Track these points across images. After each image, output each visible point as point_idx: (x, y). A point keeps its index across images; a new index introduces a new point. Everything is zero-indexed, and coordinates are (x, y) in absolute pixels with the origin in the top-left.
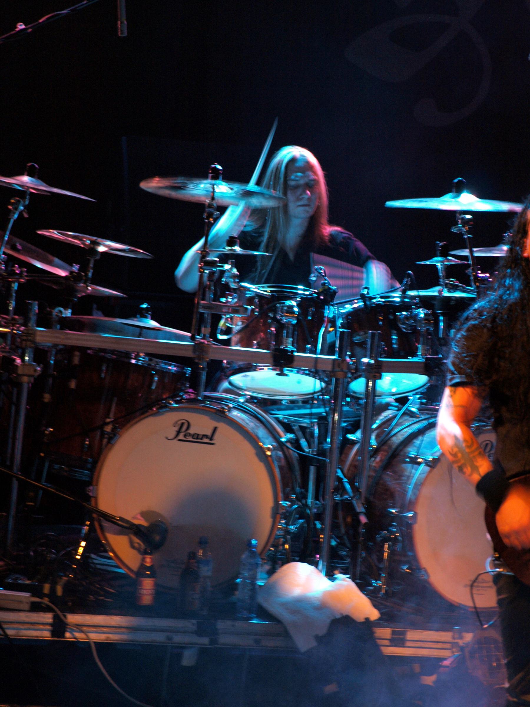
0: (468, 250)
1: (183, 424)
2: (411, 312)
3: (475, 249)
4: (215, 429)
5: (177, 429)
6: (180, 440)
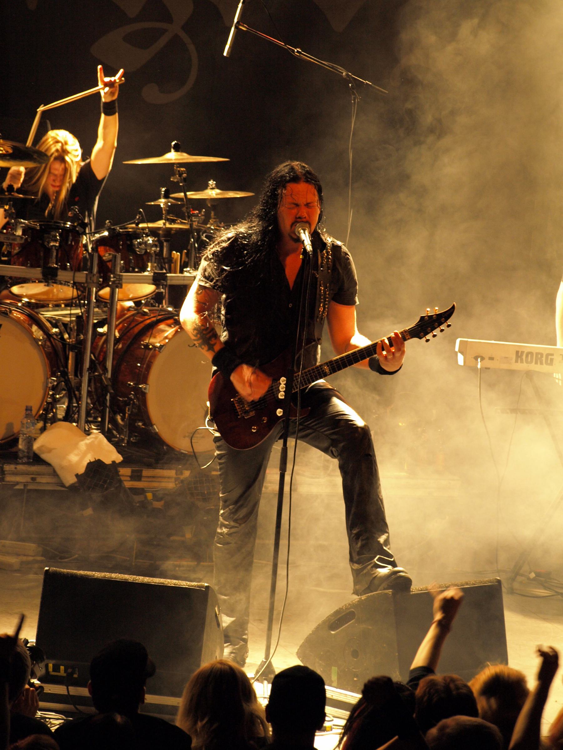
2: (143, 240)
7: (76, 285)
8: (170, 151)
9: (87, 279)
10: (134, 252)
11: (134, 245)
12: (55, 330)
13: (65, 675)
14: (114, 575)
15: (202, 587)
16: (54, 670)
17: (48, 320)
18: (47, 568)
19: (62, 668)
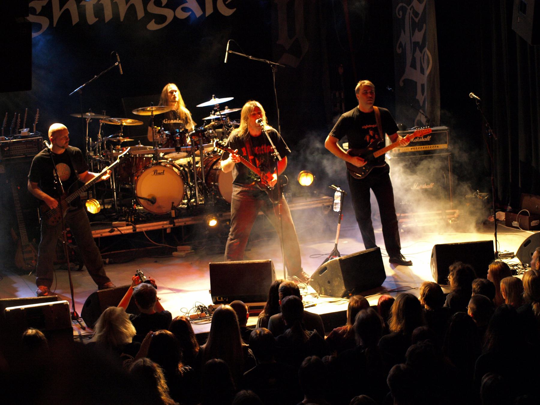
0: (219, 112)
1: (155, 171)
3: (220, 112)
4: (164, 171)
5: (154, 172)
6: (155, 175)
7: (187, 152)
8: (212, 98)
9: (191, 149)
10: (205, 137)
12: (182, 168)
13: (223, 300)
14: (235, 262)
15: (268, 261)
17: (178, 165)
18: (210, 263)
19: (222, 298)
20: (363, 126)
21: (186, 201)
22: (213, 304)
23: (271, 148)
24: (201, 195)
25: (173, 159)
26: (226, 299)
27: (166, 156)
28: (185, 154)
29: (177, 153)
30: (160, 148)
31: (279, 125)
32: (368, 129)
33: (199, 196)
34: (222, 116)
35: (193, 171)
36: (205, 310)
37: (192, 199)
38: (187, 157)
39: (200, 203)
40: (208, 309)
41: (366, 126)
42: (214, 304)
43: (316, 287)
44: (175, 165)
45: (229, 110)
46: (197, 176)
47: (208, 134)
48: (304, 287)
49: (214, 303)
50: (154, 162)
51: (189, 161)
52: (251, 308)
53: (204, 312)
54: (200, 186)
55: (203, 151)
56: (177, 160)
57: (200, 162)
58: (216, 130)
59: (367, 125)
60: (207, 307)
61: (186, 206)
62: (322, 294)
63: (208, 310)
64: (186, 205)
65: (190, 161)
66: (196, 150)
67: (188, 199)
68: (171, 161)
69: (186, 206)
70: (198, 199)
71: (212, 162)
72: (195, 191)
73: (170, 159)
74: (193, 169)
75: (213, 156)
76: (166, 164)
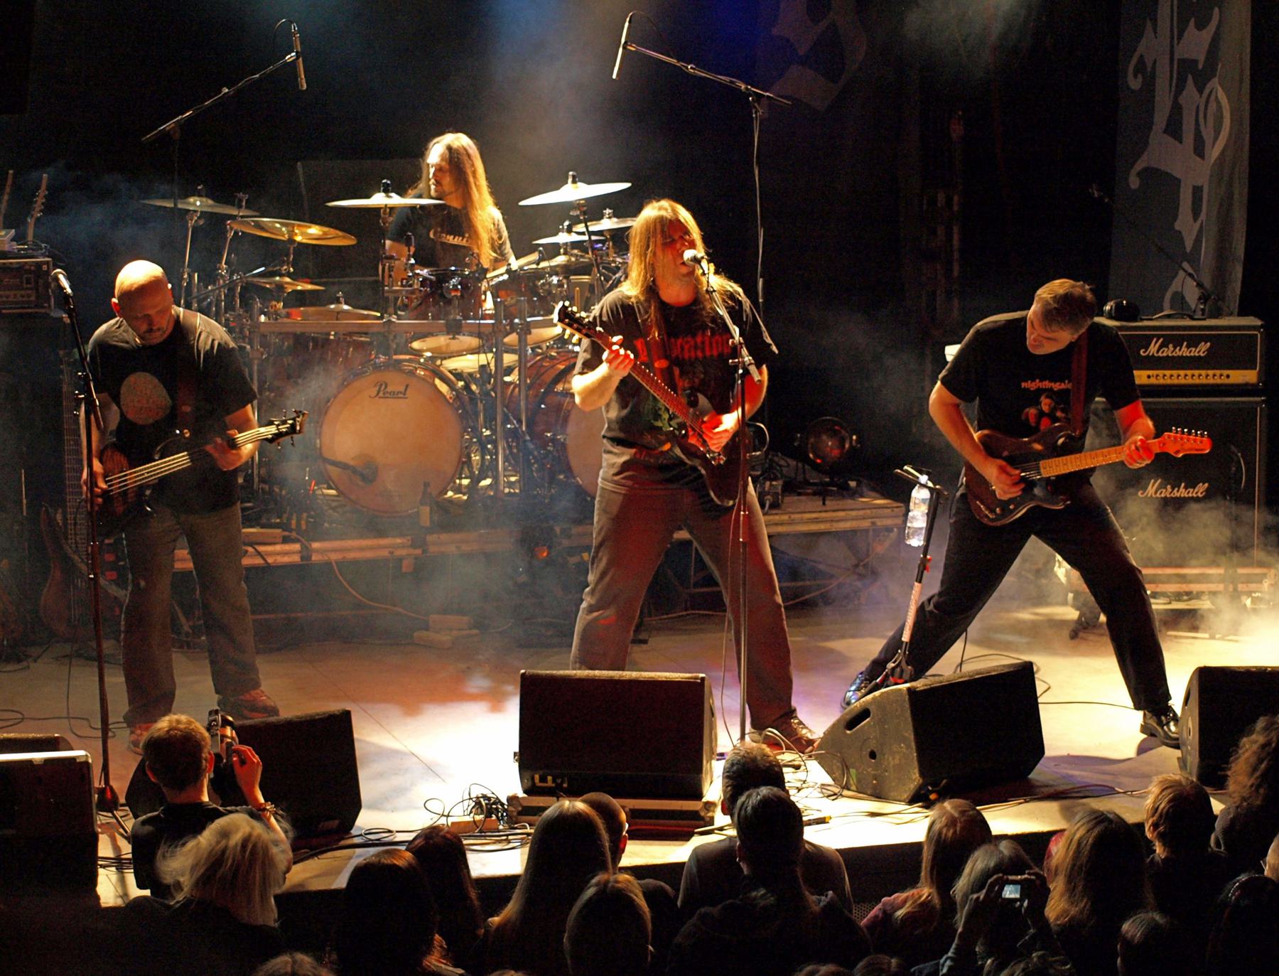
0: (583, 225)
1: (381, 385)
3: (588, 224)
4: (407, 386)
5: (377, 388)
7: (479, 336)
10: (537, 294)
11: (537, 287)
12: (461, 384)
13: (554, 785)
14: (597, 673)
15: (696, 678)
16: (540, 781)
17: (450, 372)
18: (523, 671)
19: (550, 778)
20: (1026, 381)
21: (465, 482)
22: (521, 794)
23: (731, 341)
24: (513, 467)
25: (435, 355)
26: (562, 782)
27: (416, 345)
28: (474, 342)
29: (451, 336)
30: (399, 318)
31: (761, 277)
32: (1039, 392)
33: (505, 469)
34: (594, 238)
35: (493, 394)
36: (497, 809)
37: (485, 479)
38: (478, 353)
39: (507, 490)
40: (506, 807)
41: (1034, 383)
42: (525, 795)
43: (834, 767)
44: (442, 372)
45: (615, 220)
46: (505, 409)
47: (547, 287)
48: (796, 763)
49: (525, 792)
50: (379, 358)
51: (485, 363)
52: (634, 814)
53: (494, 817)
54: (512, 442)
55: (529, 337)
56: (450, 357)
57: (516, 371)
58: (572, 277)
59: (1037, 381)
60: (505, 801)
61: (465, 498)
62: (849, 789)
63: (505, 810)
64: (464, 494)
65: (489, 364)
66: (508, 334)
67: (471, 476)
68: (432, 359)
69: (465, 498)
70: (502, 479)
71: (552, 374)
72: (497, 454)
73: (429, 354)
74: (492, 390)
75: (557, 353)
76: (416, 369)
